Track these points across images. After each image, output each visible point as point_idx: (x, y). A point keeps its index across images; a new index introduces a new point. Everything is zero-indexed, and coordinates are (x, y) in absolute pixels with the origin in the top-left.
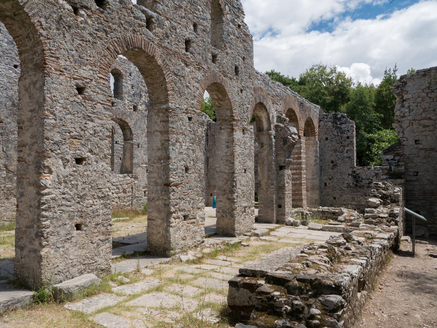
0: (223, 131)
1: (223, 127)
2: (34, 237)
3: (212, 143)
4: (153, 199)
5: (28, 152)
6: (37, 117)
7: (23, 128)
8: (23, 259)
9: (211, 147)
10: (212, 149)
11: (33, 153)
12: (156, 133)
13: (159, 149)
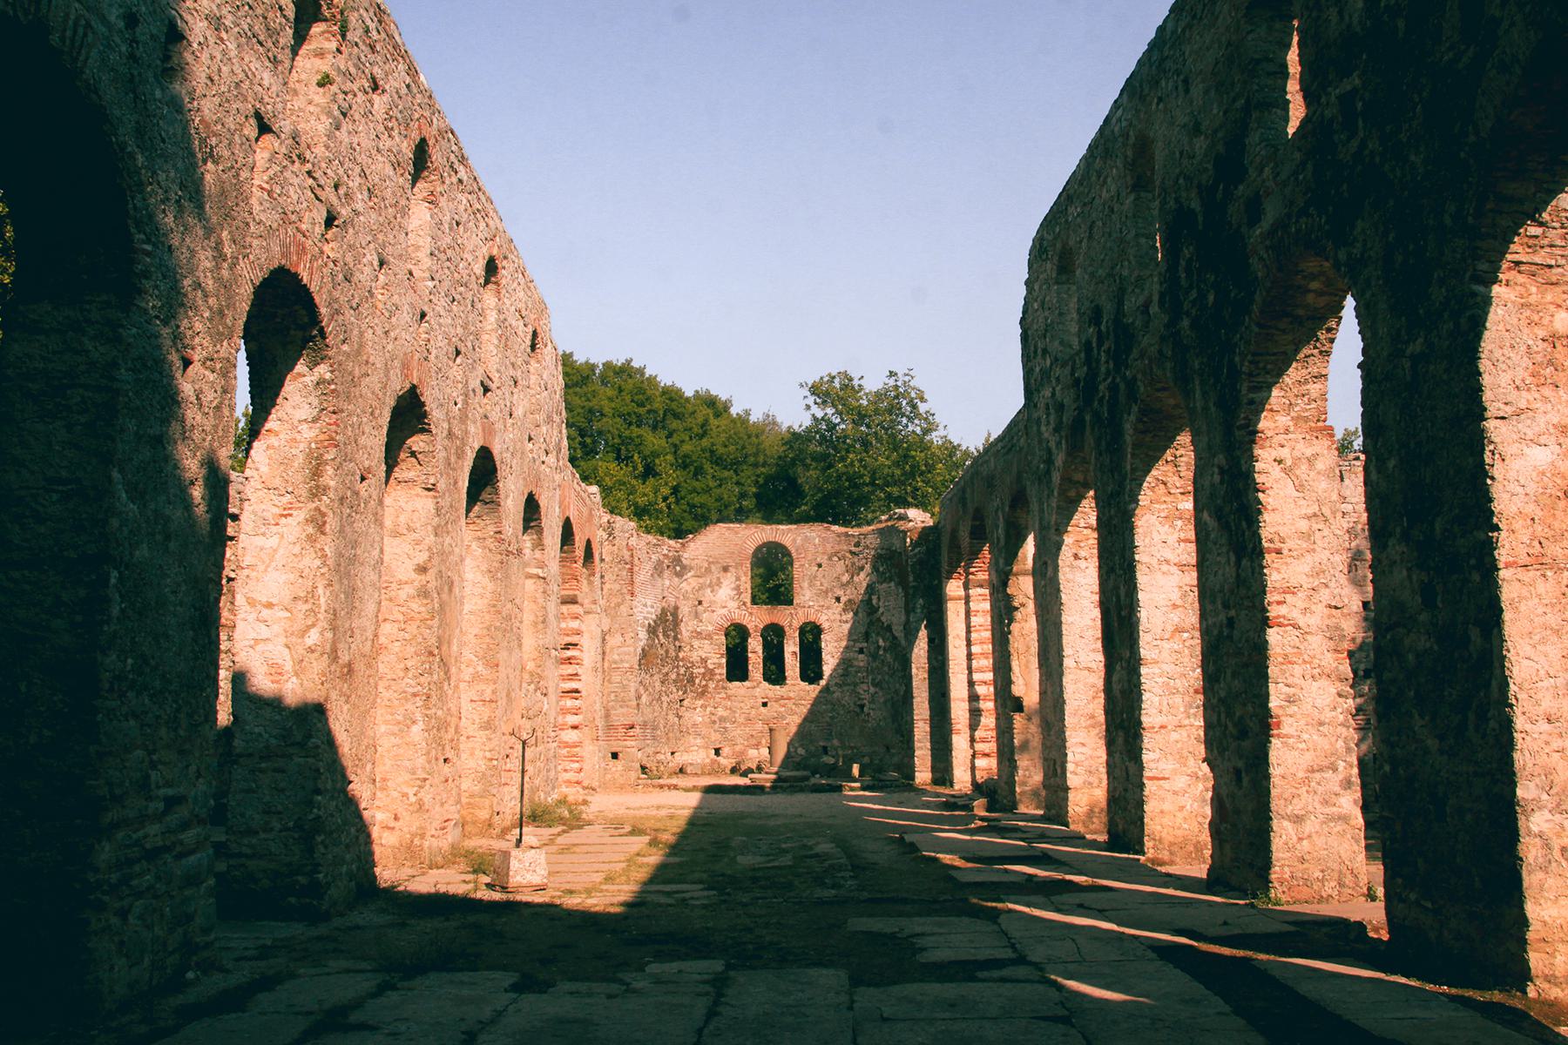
0: (1082, 564)
1: (1082, 554)
2: (1337, 789)
3: (617, 587)
4: (1162, 727)
5: (1300, 604)
6: (1326, 532)
7: (1285, 552)
8: (1305, 842)
9: (615, 600)
10: (619, 605)
11: (1320, 609)
12: (1165, 567)
13: (1175, 606)
